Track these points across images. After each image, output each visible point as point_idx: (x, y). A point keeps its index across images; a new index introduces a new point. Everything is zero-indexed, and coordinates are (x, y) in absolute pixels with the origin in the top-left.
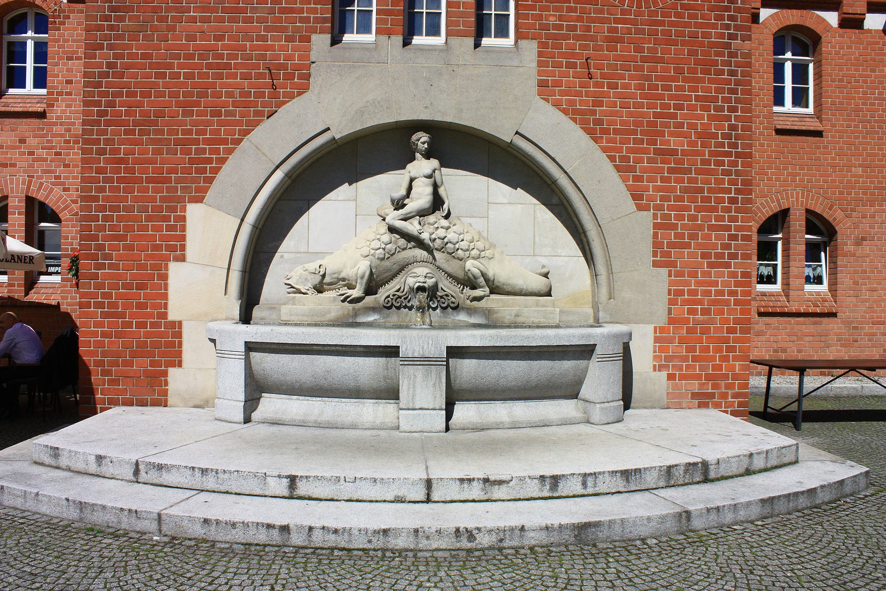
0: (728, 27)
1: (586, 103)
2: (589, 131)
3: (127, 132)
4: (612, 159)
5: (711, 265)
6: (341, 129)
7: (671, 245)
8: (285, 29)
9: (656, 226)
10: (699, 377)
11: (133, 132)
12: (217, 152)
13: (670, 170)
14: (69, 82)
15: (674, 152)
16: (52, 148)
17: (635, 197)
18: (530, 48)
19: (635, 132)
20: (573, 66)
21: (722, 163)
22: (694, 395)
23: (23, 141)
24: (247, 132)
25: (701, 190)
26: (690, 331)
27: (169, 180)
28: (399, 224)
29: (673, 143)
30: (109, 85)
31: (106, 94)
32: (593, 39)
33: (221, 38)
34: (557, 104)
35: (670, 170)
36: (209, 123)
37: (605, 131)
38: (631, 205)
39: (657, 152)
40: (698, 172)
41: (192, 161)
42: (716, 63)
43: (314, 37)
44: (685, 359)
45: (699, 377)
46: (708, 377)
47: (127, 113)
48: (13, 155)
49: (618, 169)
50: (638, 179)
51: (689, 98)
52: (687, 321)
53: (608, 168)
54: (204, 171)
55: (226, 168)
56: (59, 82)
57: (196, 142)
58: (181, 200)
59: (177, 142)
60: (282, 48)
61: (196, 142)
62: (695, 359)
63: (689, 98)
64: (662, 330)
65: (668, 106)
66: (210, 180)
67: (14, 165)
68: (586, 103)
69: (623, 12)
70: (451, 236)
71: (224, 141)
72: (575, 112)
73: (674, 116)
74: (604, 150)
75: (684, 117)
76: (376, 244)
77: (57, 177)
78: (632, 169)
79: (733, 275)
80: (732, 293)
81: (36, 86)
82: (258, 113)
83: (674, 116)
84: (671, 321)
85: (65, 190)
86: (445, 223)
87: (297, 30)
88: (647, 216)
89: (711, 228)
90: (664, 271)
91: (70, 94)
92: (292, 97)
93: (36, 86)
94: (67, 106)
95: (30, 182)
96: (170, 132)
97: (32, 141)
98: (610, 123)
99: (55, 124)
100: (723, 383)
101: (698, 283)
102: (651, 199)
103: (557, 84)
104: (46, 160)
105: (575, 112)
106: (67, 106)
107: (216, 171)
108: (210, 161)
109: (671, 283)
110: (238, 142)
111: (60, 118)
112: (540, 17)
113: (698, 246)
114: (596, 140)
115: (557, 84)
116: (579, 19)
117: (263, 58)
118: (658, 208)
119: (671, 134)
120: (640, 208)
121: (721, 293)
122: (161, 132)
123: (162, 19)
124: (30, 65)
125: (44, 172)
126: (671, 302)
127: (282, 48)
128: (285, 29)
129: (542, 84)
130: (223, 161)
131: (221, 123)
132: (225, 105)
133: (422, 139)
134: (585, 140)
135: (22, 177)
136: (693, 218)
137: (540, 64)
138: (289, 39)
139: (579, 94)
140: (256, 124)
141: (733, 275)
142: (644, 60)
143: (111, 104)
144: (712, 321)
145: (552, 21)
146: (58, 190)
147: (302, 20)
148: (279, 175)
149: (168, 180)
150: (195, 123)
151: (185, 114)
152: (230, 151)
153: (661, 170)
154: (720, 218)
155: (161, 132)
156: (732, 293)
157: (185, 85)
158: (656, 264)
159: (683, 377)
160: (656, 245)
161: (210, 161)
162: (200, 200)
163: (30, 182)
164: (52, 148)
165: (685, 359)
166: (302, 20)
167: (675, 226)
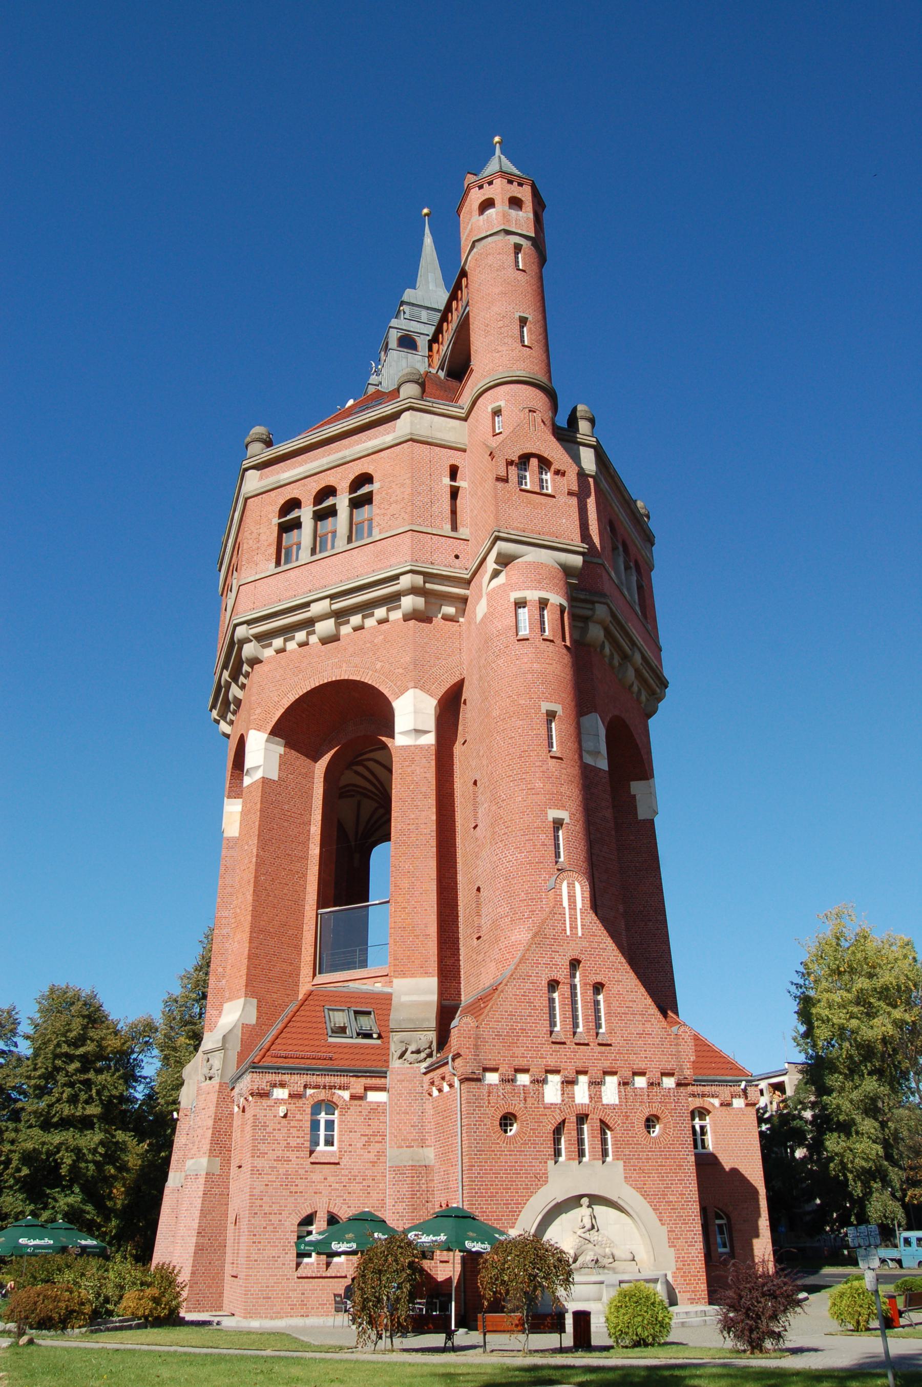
0: (686, 1151)
1: (640, 1184)
2: (643, 1195)
3: (486, 1200)
4: (651, 1206)
5: (689, 1246)
6: (560, 1199)
7: (674, 1239)
8: (538, 1159)
9: (669, 1231)
10: (689, 1291)
11: (487, 1200)
13: (671, 1209)
14: (350, 1145)
15: (672, 1202)
16: (342, 1183)
17: (661, 1220)
18: (620, 1164)
19: (658, 1195)
20: (635, 1170)
21: (688, 1205)
22: (689, 1299)
24: (527, 1200)
25: (682, 1216)
26: (684, 1272)
27: (501, 1220)
28: (583, 1235)
29: (672, 1198)
30: (478, 1181)
31: (477, 1185)
32: (641, 1159)
33: (516, 1162)
34: (631, 1185)
35: (671, 1209)
36: (515, 1196)
37: (648, 1195)
38: (658, 1223)
39: (666, 1202)
40: (681, 1209)
41: (509, 1212)
42: (683, 1166)
43: (548, 1162)
44: (683, 1284)
45: (689, 1291)
46: (693, 1291)
47: (486, 1193)
48: (321, 1187)
49: (654, 1209)
50: (660, 1213)
51: (675, 1180)
52: (682, 1269)
53: (650, 1209)
54: (514, 1215)
55: (522, 1214)
56: (345, 1145)
57: (510, 1204)
58: (506, 1227)
59: (504, 1204)
60: (538, 1166)
61: (510, 1204)
62: (687, 1284)
63: (675, 1180)
64: (674, 1273)
65: (667, 1184)
66: (516, 1219)
67: (320, 1193)
68: (640, 1184)
69: (651, 1148)
71: (520, 1204)
72: (638, 1188)
73: (671, 1188)
74: (649, 1202)
75: (674, 1188)
76: (574, 1243)
77: (344, 1200)
79: (697, 1249)
80: (697, 1257)
82: (532, 1192)
83: (671, 1188)
84: (677, 1269)
85: (348, 1207)
86: (596, 1234)
87: (542, 1159)
88: (665, 1227)
89: (687, 1231)
90: (673, 1249)
92: (542, 1185)
95: (329, 1203)
96: (501, 1200)
97: (331, 1179)
98: (650, 1192)
99: (343, 1169)
100: (698, 1294)
101: (685, 1253)
102: (665, 1220)
103: (631, 1177)
105: (638, 1188)
107: (518, 1215)
108: (516, 1212)
109: (676, 1254)
110: (525, 1204)
111: (345, 1165)
112: (622, 1152)
113: (684, 1238)
114: (645, 1199)
115: (631, 1177)
116: (636, 1152)
117: (532, 1170)
118: (668, 1224)
119: (671, 1195)
120: (662, 1224)
121: (693, 1257)
122: (498, 1200)
123: (495, 1155)
124: (322, 1133)
125: (337, 1196)
126: (677, 1261)
127: (538, 1166)
128: (538, 1159)
129: (626, 1177)
130: (520, 1211)
131: (519, 1196)
132: (520, 1189)
133: (585, 1201)
134: (641, 1198)
135: (326, 1199)
136: (681, 1227)
137: (625, 1170)
138: (540, 1163)
139: (638, 1181)
140: (531, 1196)
141: (697, 1249)
142: (659, 1166)
143: (479, 1189)
144: (692, 1268)
146: (345, 1207)
147: (544, 1155)
148: (540, 1217)
149: (501, 1220)
150: (509, 1196)
151: (506, 1193)
152: (523, 1207)
153: (668, 1209)
154: (690, 1227)
155: (498, 1200)
156: (697, 1257)
157: (505, 1181)
158: (670, 1247)
159: (684, 1292)
160: (669, 1239)
161: (516, 1212)
162: (513, 1227)
163: (329, 1203)
164: (342, 1183)
165: (683, 1284)
166: (544, 1155)
167: (675, 1231)
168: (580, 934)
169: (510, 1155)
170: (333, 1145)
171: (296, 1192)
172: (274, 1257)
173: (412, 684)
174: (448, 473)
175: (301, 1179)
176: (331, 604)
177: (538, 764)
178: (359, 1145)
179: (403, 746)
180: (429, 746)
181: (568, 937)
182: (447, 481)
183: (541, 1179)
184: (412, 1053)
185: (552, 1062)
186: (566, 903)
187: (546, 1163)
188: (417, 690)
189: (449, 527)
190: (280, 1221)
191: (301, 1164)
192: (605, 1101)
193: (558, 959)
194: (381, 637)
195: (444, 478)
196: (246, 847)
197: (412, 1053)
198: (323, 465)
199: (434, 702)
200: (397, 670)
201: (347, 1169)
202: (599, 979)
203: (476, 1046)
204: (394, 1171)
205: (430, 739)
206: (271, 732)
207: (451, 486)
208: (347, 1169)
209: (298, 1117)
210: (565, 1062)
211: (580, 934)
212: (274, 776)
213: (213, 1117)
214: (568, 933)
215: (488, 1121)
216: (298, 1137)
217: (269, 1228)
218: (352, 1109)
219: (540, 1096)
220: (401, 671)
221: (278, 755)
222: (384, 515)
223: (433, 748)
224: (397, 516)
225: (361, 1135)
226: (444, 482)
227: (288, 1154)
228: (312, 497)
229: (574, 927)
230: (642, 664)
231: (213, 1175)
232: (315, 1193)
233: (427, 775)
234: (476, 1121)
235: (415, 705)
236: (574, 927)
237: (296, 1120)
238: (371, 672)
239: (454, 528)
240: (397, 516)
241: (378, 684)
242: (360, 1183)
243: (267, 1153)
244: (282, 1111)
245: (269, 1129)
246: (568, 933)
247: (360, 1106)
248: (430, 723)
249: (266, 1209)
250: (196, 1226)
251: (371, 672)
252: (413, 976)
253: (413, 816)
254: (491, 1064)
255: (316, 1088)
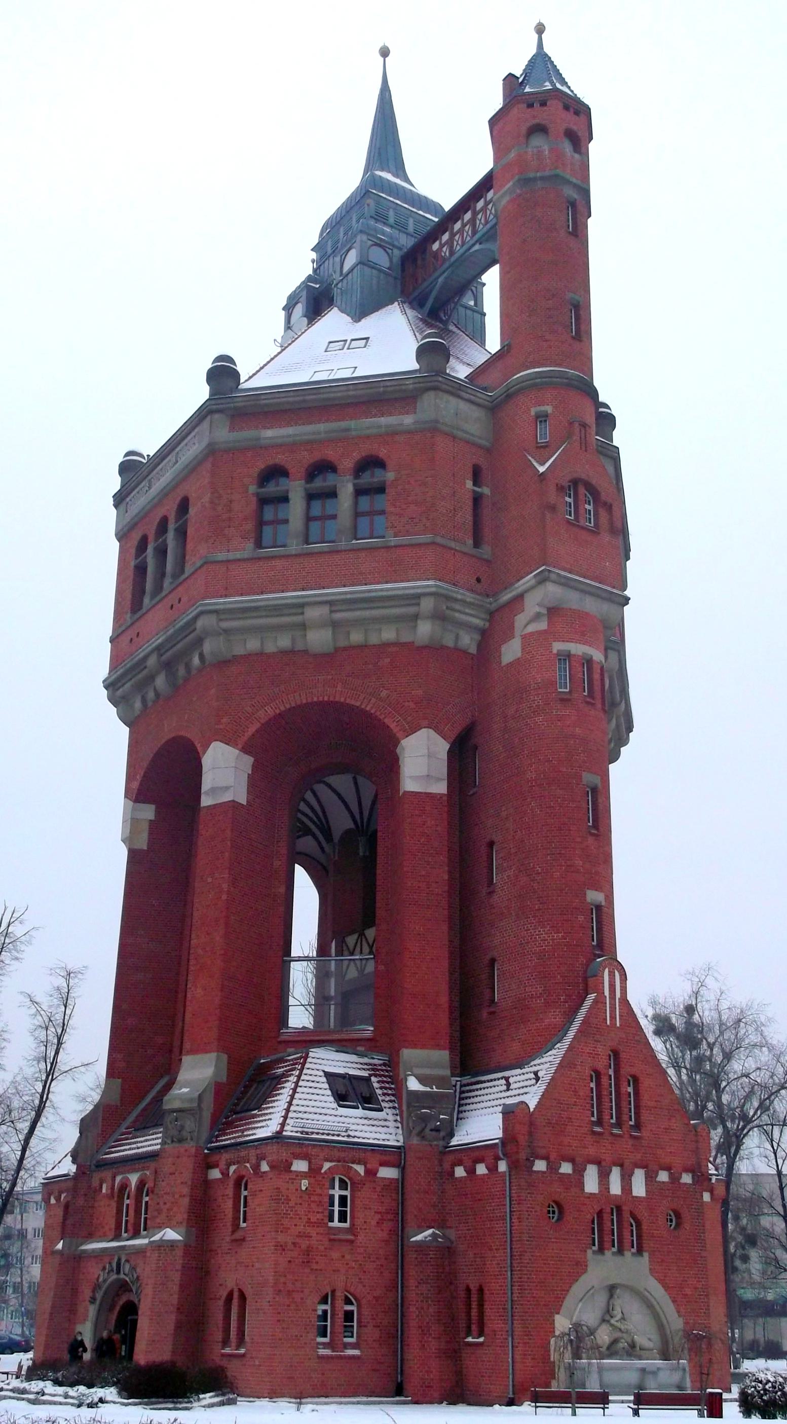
2: (663, 1286)
12: (562, 1294)
17: (678, 1312)
23: (343, 1257)
29: (688, 1291)
50: (678, 1305)
53: (670, 1301)
57: (556, 1290)
61: (556, 1290)
70: (629, 1328)
71: (564, 1291)
78: (676, 1301)
81: (340, 1221)
91: (365, 1229)
92: (583, 1273)
93: (340, 1221)
94: (365, 1236)
97: (348, 1257)
104: (354, 1268)
106: (365, 1236)
107: (562, 1302)
118: (685, 1316)
124: (336, 1208)
130: (564, 1298)
135: (343, 1278)
143: (530, 1274)
145: (652, 1245)
146: (360, 1286)
162: (558, 1313)
168: (618, 1025)
169: (556, 1242)
170: (346, 1222)
171: (316, 1270)
172: (296, 1336)
173: (426, 722)
174: (470, 475)
175: (321, 1256)
176: (331, 612)
177: (579, 840)
178: (374, 1223)
179: (412, 792)
180: (442, 795)
181: (608, 1026)
182: (469, 484)
183: (580, 1267)
184: (431, 1130)
185: (592, 1151)
186: (607, 993)
187: (586, 1251)
188: (430, 730)
189: (470, 542)
190: (302, 1299)
191: (321, 1241)
192: (635, 1193)
193: (600, 1049)
194: (387, 660)
195: (468, 481)
196: (210, 880)
197: (431, 1130)
198: (319, 433)
199: (447, 746)
200: (407, 704)
201: (362, 1247)
202: (634, 1071)
203: (530, 1134)
204: (416, 1251)
205: (441, 788)
206: (243, 748)
207: (474, 491)
208: (362, 1247)
209: (319, 1191)
210: (604, 1153)
211: (618, 1025)
212: (243, 799)
213: (190, 1183)
214: (608, 1023)
215: (538, 1208)
216: (318, 1212)
217: (293, 1307)
218: (367, 1185)
219: (581, 1185)
220: (412, 705)
221: (247, 776)
222: (400, 515)
223: (445, 798)
224: (417, 520)
225: (375, 1212)
226: (468, 486)
227: (309, 1230)
228: (303, 470)
229: (613, 1018)
230: (447, 608)
231: (190, 1246)
232: (334, 1271)
233: (439, 828)
234: (528, 1207)
235: (428, 749)
236: (613, 1018)
237: (317, 1195)
238: (374, 700)
239: (477, 544)
240: (417, 520)
241: (383, 716)
242: (374, 1262)
243: (289, 1228)
244: (304, 1184)
245: (291, 1204)
246: (608, 1023)
247: (375, 1182)
248: (442, 769)
249: (290, 1286)
250: (175, 1302)
251: (374, 700)
252: (423, 1047)
253: (423, 873)
254: (543, 1152)
255: (339, 1161)
